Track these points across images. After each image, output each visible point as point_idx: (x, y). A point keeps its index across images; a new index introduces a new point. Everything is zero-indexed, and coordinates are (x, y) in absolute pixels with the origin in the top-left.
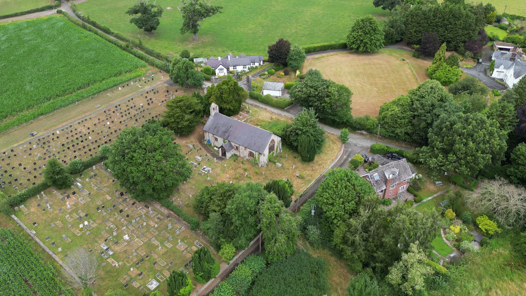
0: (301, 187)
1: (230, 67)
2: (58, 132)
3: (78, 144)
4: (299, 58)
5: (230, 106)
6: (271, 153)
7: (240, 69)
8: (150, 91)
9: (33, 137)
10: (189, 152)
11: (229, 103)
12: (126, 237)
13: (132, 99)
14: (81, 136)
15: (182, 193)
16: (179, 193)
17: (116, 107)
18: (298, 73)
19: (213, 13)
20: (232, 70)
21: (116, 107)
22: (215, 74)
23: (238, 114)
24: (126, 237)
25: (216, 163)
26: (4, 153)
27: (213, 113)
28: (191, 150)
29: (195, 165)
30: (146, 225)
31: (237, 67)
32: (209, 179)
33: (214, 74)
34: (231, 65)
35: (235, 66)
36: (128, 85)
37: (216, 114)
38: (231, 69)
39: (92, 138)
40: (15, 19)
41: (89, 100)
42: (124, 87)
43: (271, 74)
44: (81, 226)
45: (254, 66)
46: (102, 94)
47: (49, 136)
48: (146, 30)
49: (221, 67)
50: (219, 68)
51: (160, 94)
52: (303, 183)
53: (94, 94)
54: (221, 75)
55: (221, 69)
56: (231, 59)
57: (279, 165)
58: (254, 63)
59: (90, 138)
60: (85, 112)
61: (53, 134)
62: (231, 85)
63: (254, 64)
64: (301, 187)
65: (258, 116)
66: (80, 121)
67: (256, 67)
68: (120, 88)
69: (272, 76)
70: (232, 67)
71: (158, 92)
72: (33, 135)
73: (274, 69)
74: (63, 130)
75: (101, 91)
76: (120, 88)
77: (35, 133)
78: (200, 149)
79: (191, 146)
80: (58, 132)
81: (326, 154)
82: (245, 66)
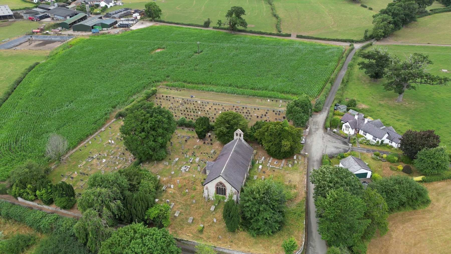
0: (186, 235)
1: (360, 131)
2: (199, 102)
3: (190, 112)
4: (429, 162)
5: (266, 146)
6: (221, 196)
7: (369, 137)
8: (277, 112)
9: (191, 98)
10: (204, 153)
11: (268, 142)
12: (104, 160)
13: (258, 109)
14: (199, 110)
15: (153, 167)
16: (152, 166)
17: (243, 108)
18: (419, 178)
19: (441, 83)
20: (362, 134)
21: (243, 108)
22: (341, 128)
23: (277, 159)
24: (104, 160)
25: (198, 171)
26: (170, 97)
27: (235, 137)
28: (207, 154)
29: (190, 162)
30: (117, 164)
31: (367, 134)
32: (173, 173)
33: (341, 127)
34: (362, 128)
35: (366, 132)
36: (277, 101)
37: (237, 139)
38: (361, 133)
39: (200, 114)
40: (314, 41)
41: (244, 97)
42: (272, 101)
43: (388, 160)
44: (110, 141)
45: (390, 144)
46: (256, 98)
47: (193, 101)
48: (371, 76)
49: (347, 124)
50: (346, 124)
51: (280, 116)
52: (192, 234)
53: (250, 96)
54: (346, 132)
55: (346, 127)
56: (367, 123)
57: (213, 208)
58: (392, 141)
59: (200, 113)
60: (229, 101)
61: (196, 102)
62: (276, 129)
63: (392, 143)
64: (186, 235)
65: (287, 173)
66: (215, 103)
67: (392, 147)
68: (269, 100)
69: (387, 162)
70: (362, 132)
71: (279, 114)
72: (192, 97)
73: (399, 158)
74: (202, 102)
75: (257, 96)
76: (269, 100)
77: (194, 97)
78: (212, 157)
79: (212, 152)
80: (199, 102)
81: (256, 243)
82: (375, 138)
